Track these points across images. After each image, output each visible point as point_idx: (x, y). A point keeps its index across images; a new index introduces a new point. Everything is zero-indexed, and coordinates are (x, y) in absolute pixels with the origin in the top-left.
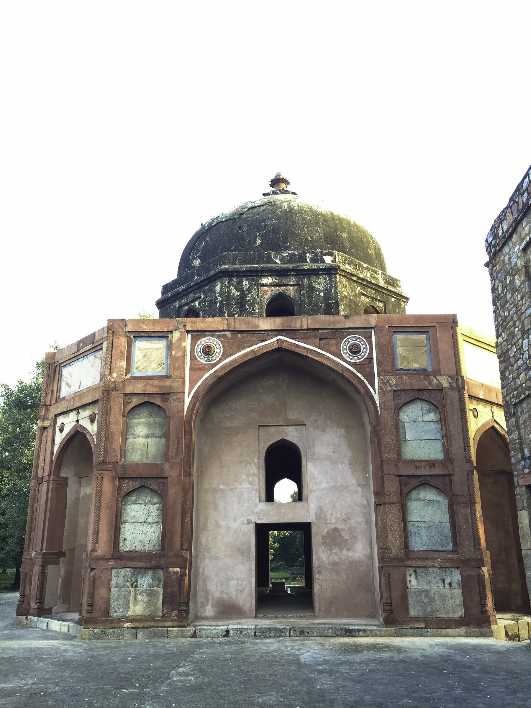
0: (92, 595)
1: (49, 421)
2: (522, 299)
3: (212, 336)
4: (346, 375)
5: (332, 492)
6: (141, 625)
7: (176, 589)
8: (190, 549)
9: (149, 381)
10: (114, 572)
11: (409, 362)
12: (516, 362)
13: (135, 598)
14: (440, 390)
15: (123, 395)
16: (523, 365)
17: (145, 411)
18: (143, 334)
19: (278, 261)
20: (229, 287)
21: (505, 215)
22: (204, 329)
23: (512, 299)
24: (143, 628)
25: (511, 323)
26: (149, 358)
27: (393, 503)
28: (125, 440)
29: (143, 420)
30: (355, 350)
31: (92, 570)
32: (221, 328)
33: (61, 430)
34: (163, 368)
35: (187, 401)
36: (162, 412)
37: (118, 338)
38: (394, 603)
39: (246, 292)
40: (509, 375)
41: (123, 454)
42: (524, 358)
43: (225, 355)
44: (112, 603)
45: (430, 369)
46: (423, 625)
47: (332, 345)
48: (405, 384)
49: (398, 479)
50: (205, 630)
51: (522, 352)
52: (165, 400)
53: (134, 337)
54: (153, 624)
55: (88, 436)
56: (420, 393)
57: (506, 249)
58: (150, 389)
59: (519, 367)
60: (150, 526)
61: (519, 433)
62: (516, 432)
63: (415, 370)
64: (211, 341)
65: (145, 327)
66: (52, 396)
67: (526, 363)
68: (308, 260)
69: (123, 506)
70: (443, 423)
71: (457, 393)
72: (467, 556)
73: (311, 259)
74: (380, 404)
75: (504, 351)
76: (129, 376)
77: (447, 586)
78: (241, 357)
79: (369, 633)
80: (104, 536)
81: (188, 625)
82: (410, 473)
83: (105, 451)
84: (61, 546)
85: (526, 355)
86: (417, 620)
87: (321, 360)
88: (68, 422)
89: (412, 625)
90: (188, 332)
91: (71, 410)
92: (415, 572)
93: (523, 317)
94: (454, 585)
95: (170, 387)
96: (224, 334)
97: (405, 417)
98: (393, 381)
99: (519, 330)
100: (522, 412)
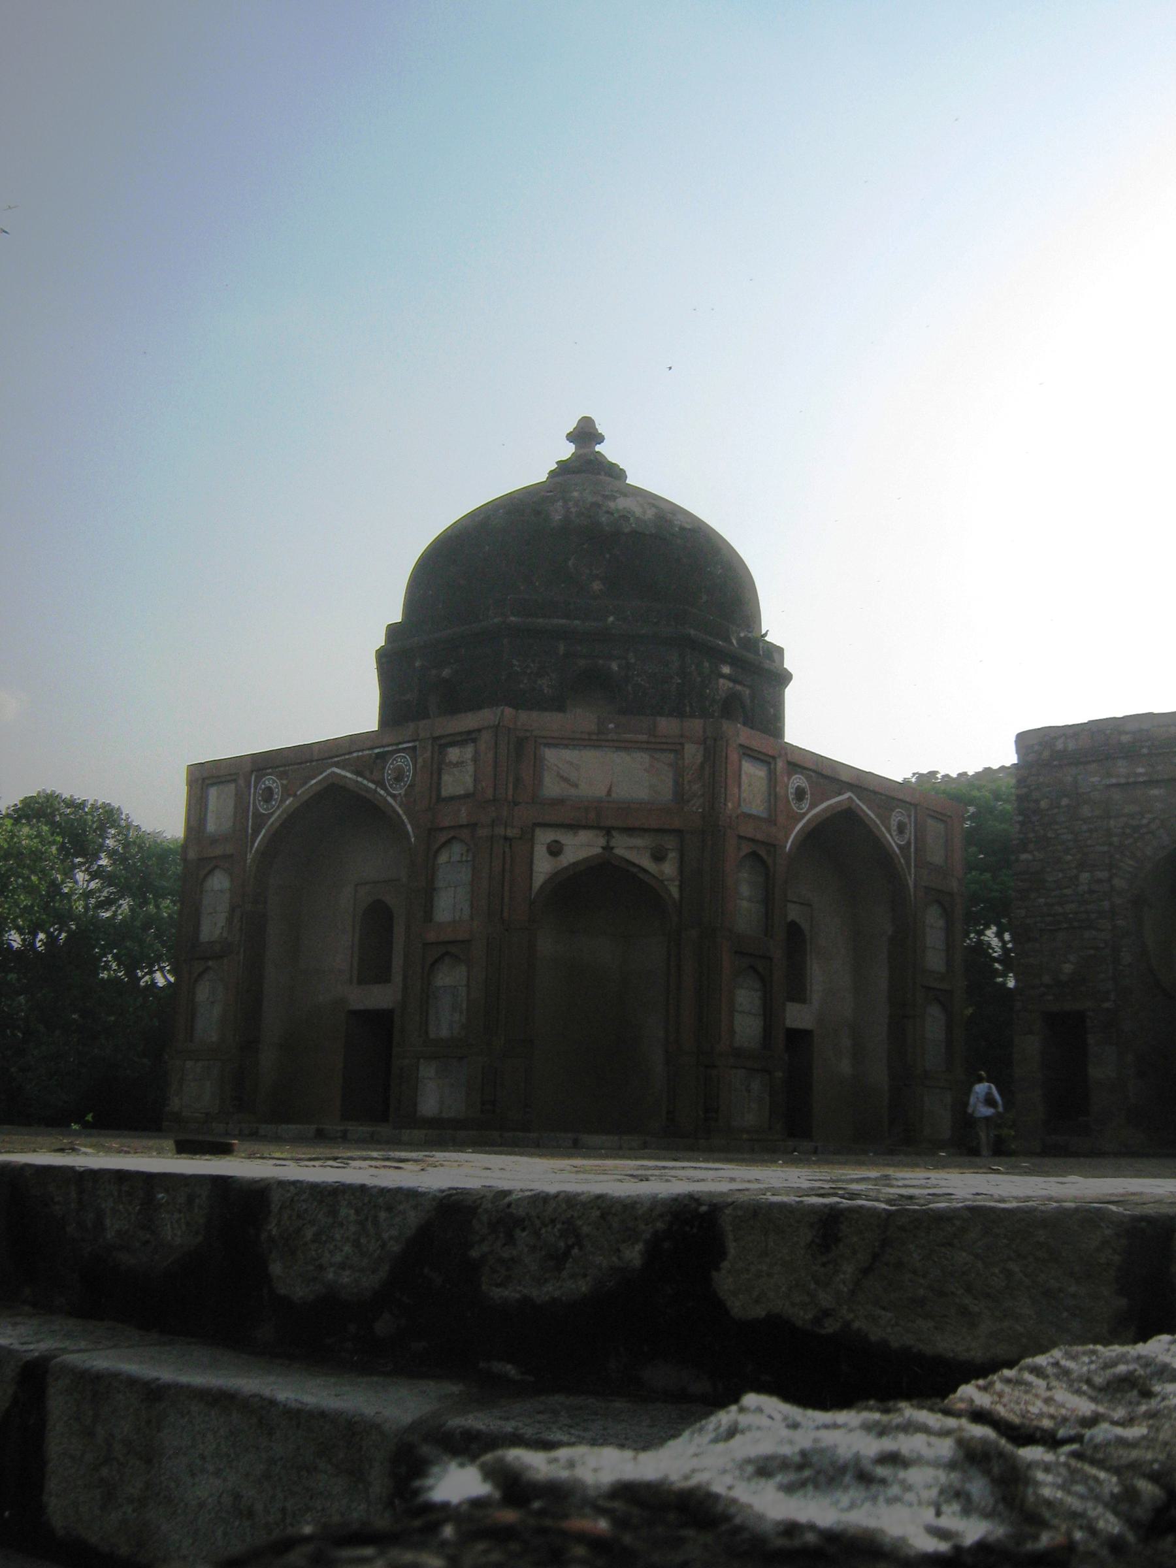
3: (802, 774)
19: (735, 642)
30: (901, 829)
43: (813, 806)
58: (759, 836)
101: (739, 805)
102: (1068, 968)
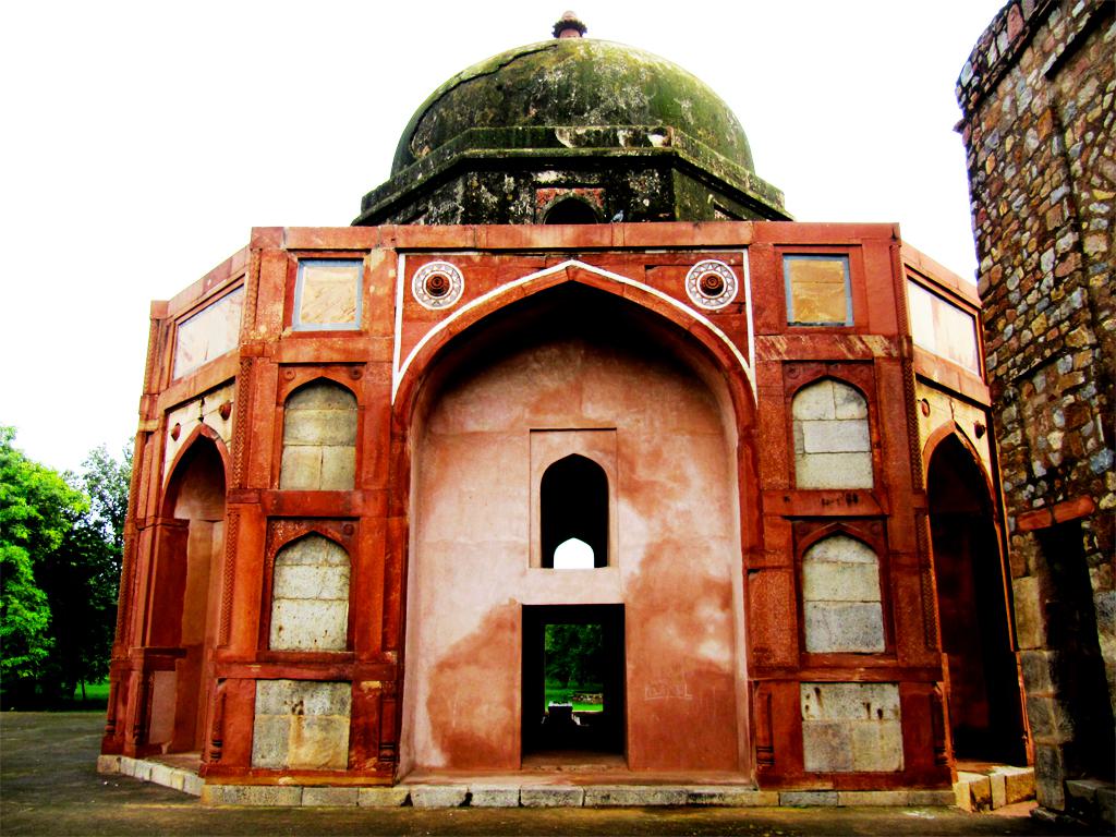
0: (220, 726)
1: (157, 422)
2: (1041, 173)
3: (446, 259)
4: (696, 332)
5: (678, 529)
6: (311, 781)
7: (374, 719)
8: (400, 649)
9: (326, 340)
10: (260, 684)
11: (811, 311)
12: (1024, 297)
13: (300, 730)
14: (868, 361)
15: (277, 366)
16: (1039, 300)
17: (318, 397)
18: (317, 255)
20: (479, 188)
21: (1005, 21)
22: (430, 246)
23: (1017, 179)
24: (313, 786)
25: (1014, 226)
26: (328, 301)
27: (780, 568)
28: (279, 446)
29: (313, 412)
30: (712, 287)
31: (221, 681)
32: (462, 245)
33: (175, 436)
34: (353, 318)
35: (398, 377)
36: (349, 398)
37: (270, 261)
38: (777, 747)
39: (510, 198)
40: (1006, 326)
41: (277, 473)
42: (1043, 287)
43: (468, 295)
44: (256, 741)
45: (849, 322)
46: (829, 786)
47: (670, 278)
48: (804, 350)
49: (789, 523)
50: (427, 793)
51: (1039, 276)
52: (356, 376)
53: (300, 260)
54: (331, 780)
55: (217, 443)
56: (832, 367)
57: (1007, 85)
58: (327, 356)
59: (1031, 306)
60: (327, 606)
61: (1024, 434)
62: (1019, 432)
63: (822, 325)
64: (443, 269)
65: (320, 242)
66: (161, 378)
67: (1049, 295)
68: (622, 142)
69: (276, 569)
70: (873, 421)
71: (898, 368)
72: (913, 662)
73: (627, 140)
74: (758, 386)
75: (995, 282)
76: (288, 332)
77: (874, 715)
78: (499, 298)
79: (728, 800)
80: (242, 623)
81: (397, 783)
82: (812, 512)
83: (245, 468)
84: (178, 636)
85: (1049, 280)
86: (819, 776)
87: (648, 304)
88: (187, 422)
89: (809, 785)
90: (399, 251)
91: (191, 400)
92: (818, 691)
93: (1042, 208)
94: (887, 714)
95: (365, 352)
96: (469, 258)
97: (804, 412)
98: (782, 343)
99: (1031, 236)
100: (1033, 393)
101: (287, 321)
102: (1056, 440)
